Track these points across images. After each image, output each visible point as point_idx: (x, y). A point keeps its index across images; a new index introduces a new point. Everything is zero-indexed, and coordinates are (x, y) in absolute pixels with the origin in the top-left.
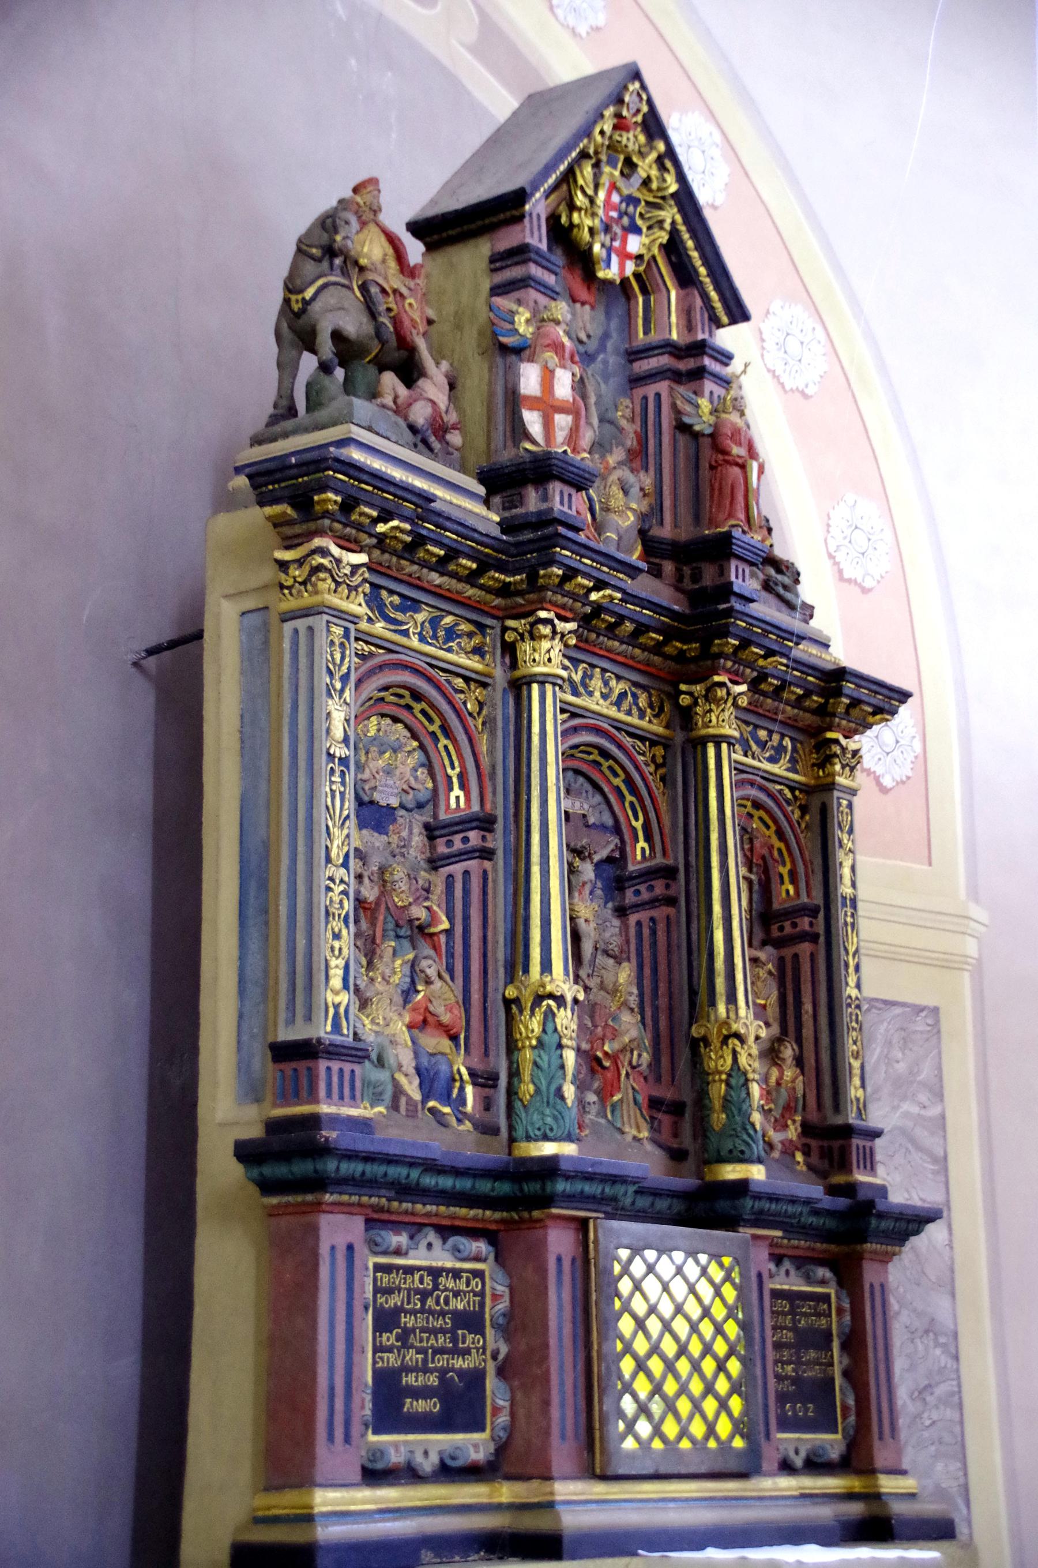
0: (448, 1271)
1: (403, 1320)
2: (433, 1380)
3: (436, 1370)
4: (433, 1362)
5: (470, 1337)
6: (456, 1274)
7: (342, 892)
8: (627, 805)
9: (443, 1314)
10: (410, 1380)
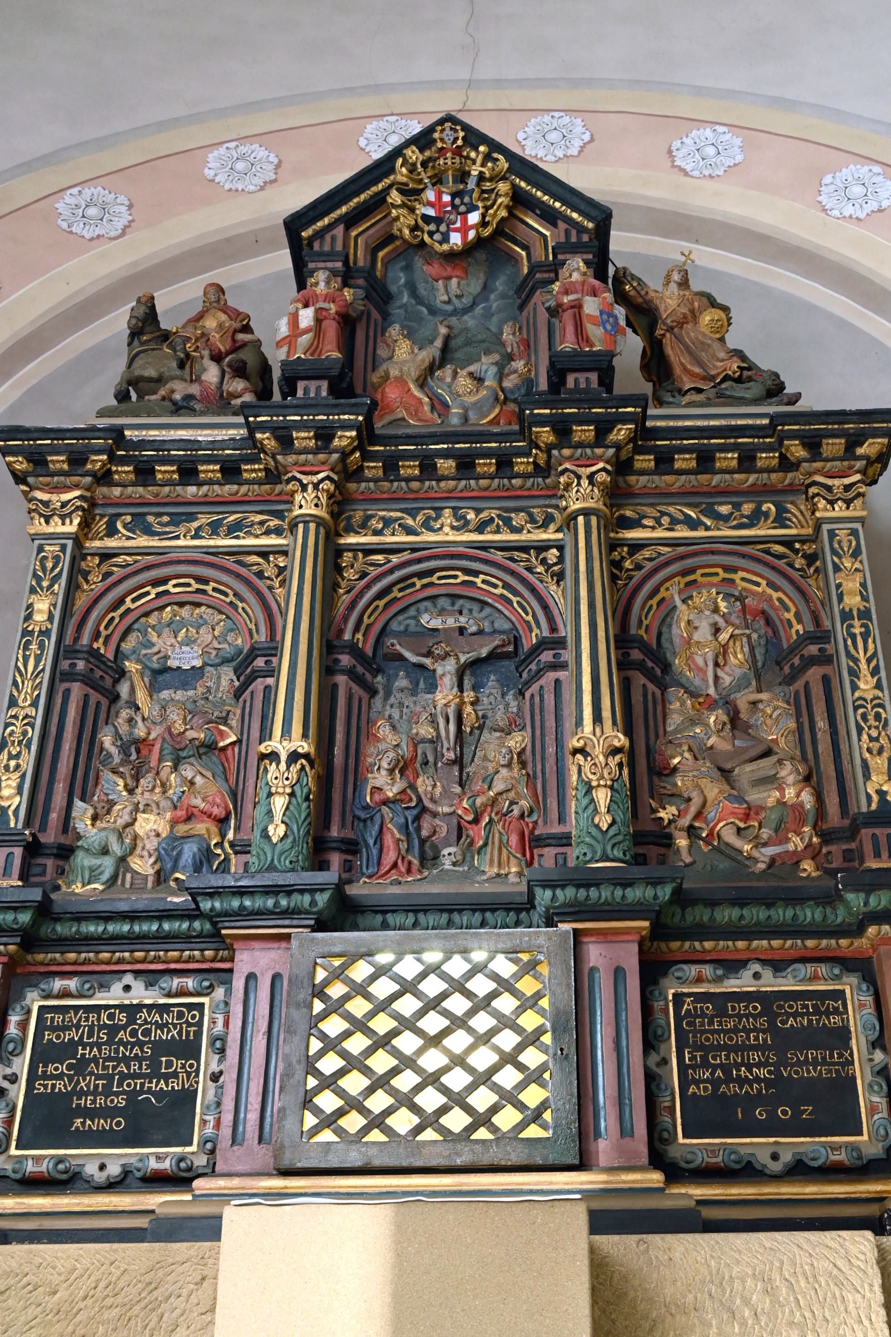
0: (150, 1007)
1: (80, 1052)
2: (121, 1102)
3: (124, 1092)
4: (120, 1085)
5: (177, 1064)
8: (515, 605)
9: (141, 1045)
10: (87, 1102)
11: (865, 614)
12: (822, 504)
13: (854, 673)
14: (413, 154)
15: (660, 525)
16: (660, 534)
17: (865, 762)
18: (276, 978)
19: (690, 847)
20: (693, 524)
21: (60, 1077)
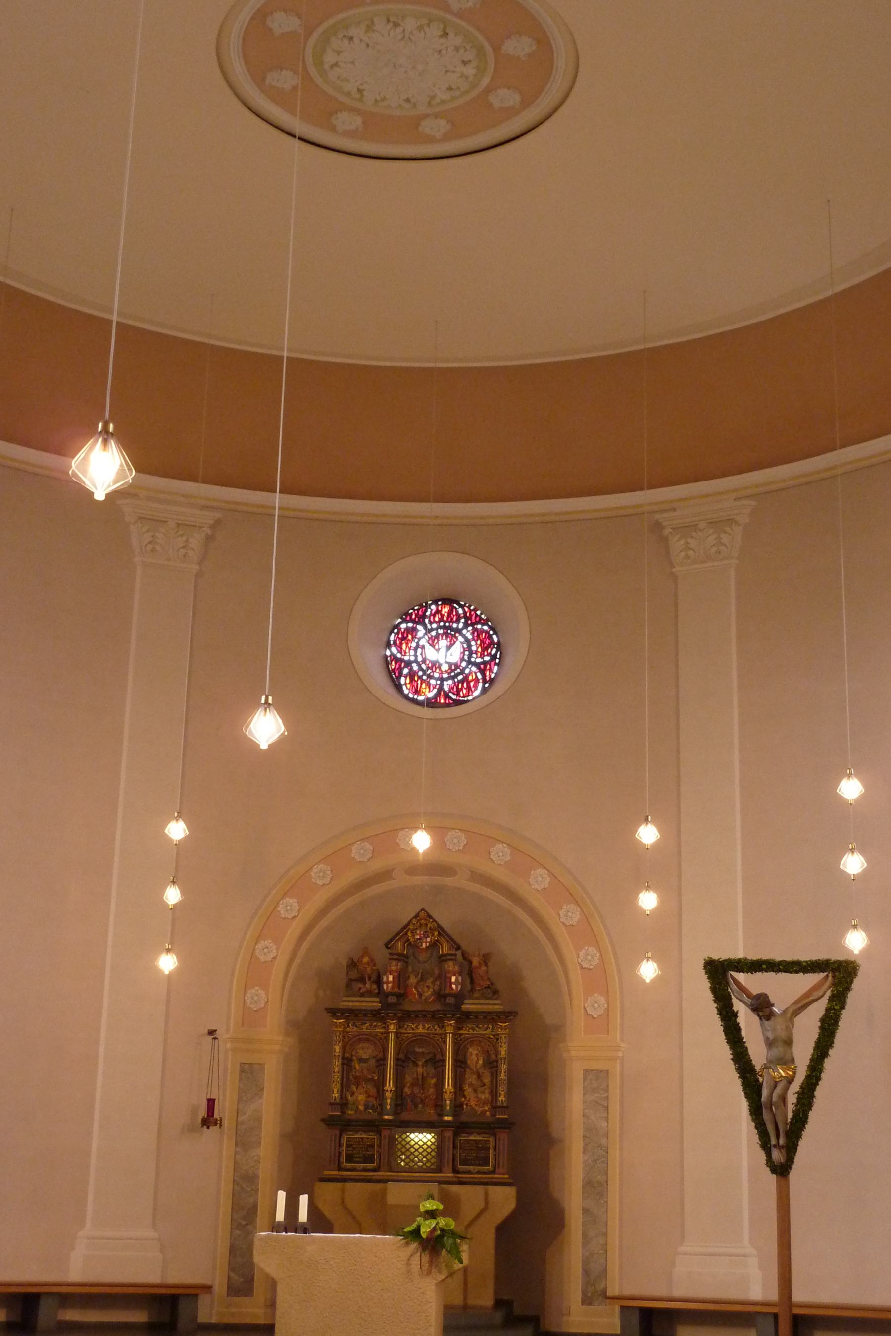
2: (361, 1155)
6: (368, 1138)
7: (338, 1078)
10: (356, 1155)
11: (505, 1058)
12: (500, 1030)
13: (501, 1072)
14: (414, 921)
15: (466, 1029)
16: (466, 1032)
17: (500, 1094)
18: (389, 1136)
19: (466, 1108)
20: (473, 1029)
21: (351, 1150)
